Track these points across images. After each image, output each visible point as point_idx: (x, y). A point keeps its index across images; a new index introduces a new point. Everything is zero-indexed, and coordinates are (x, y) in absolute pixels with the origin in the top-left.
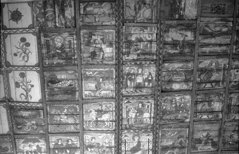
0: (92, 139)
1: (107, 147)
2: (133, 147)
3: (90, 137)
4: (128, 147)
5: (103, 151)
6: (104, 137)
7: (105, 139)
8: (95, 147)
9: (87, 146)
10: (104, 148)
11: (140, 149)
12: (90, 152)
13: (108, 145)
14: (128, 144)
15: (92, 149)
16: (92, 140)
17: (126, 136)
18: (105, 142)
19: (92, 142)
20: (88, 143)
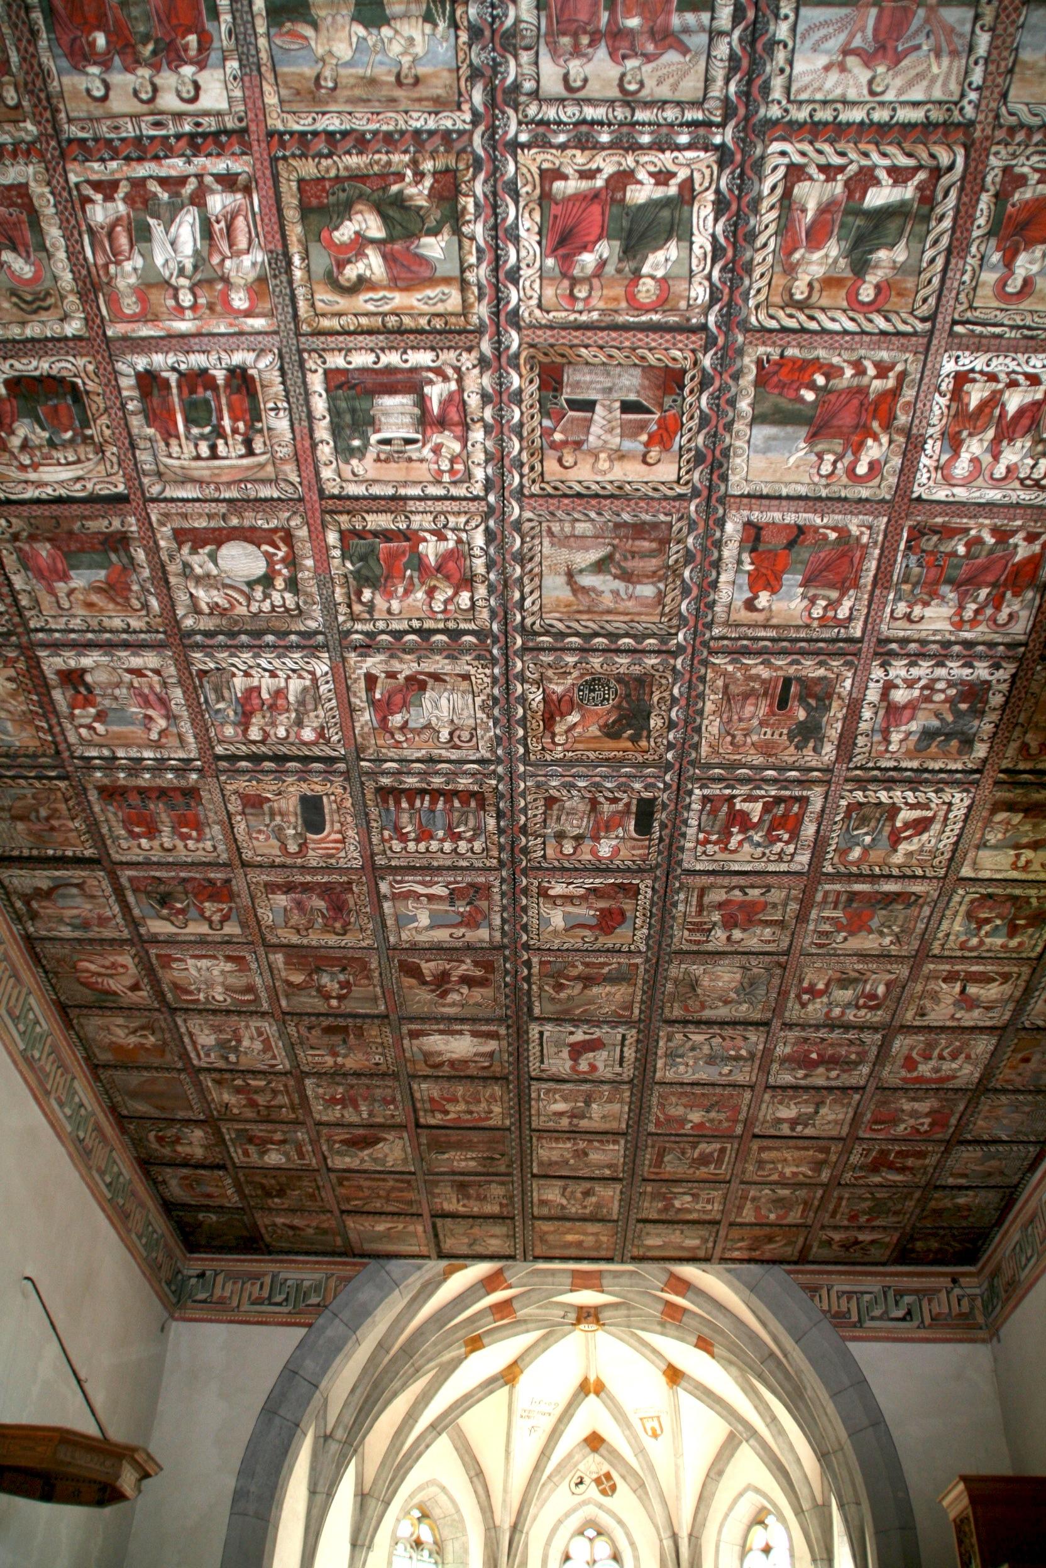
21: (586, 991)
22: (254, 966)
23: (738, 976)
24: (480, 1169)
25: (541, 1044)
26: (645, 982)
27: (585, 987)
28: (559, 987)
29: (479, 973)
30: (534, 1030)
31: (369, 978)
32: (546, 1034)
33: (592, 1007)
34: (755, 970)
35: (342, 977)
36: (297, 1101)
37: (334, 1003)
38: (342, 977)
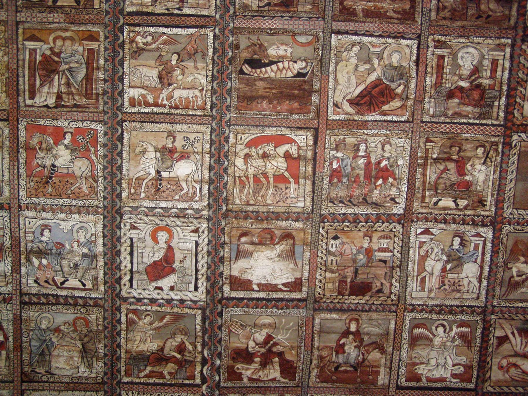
0: (43, 230)
1: (85, 256)
2: (154, 261)
3: (38, 224)
4: (140, 260)
5: (72, 266)
6: (74, 225)
7: (78, 232)
8: (52, 254)
9: (30, 251)
10: (77, 259)
11: (173, 271)
12: (39, 268)
13: (85, 250)
14: (140, 251)
15: (44, 262)
16: (42, 235)
17: (134, 227)
18: (78, 241)
19: (44, 239)
20: (32, 241)
21: (161, 344)
22: (403, 370)
23: (54, 365)
24: (265, 39)
25: (197, 271)
26: (119, 358)
27: (162, 349)
28: (181, 349)
29: (239, 366)
30: (201, 295)
31: (321, 358)
32: (192, 287)
33: (156, 324)
34: (42, 371)
35: (341, 359)
36: (419, 170)
37: (353, 327)
38: (341, 359)
